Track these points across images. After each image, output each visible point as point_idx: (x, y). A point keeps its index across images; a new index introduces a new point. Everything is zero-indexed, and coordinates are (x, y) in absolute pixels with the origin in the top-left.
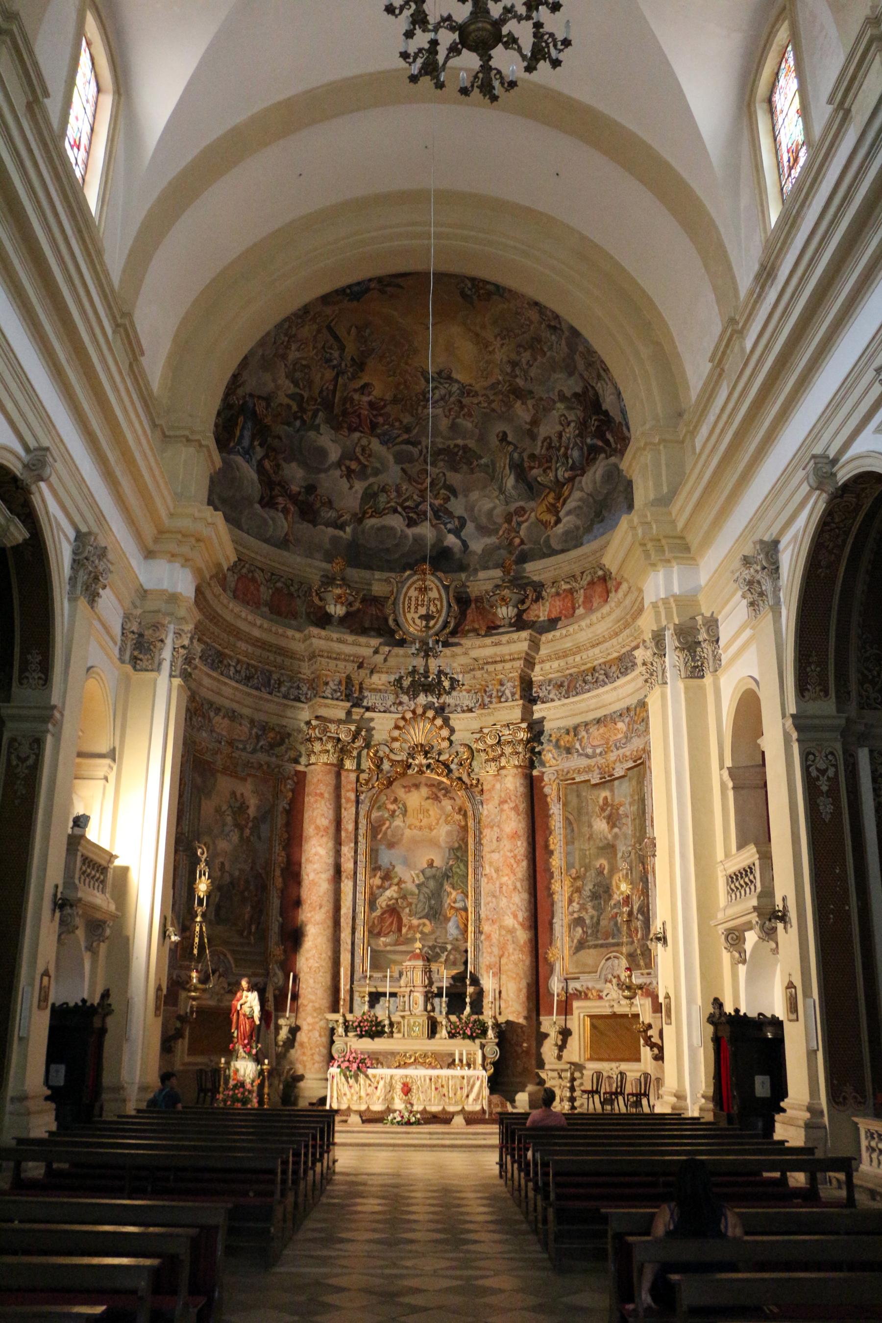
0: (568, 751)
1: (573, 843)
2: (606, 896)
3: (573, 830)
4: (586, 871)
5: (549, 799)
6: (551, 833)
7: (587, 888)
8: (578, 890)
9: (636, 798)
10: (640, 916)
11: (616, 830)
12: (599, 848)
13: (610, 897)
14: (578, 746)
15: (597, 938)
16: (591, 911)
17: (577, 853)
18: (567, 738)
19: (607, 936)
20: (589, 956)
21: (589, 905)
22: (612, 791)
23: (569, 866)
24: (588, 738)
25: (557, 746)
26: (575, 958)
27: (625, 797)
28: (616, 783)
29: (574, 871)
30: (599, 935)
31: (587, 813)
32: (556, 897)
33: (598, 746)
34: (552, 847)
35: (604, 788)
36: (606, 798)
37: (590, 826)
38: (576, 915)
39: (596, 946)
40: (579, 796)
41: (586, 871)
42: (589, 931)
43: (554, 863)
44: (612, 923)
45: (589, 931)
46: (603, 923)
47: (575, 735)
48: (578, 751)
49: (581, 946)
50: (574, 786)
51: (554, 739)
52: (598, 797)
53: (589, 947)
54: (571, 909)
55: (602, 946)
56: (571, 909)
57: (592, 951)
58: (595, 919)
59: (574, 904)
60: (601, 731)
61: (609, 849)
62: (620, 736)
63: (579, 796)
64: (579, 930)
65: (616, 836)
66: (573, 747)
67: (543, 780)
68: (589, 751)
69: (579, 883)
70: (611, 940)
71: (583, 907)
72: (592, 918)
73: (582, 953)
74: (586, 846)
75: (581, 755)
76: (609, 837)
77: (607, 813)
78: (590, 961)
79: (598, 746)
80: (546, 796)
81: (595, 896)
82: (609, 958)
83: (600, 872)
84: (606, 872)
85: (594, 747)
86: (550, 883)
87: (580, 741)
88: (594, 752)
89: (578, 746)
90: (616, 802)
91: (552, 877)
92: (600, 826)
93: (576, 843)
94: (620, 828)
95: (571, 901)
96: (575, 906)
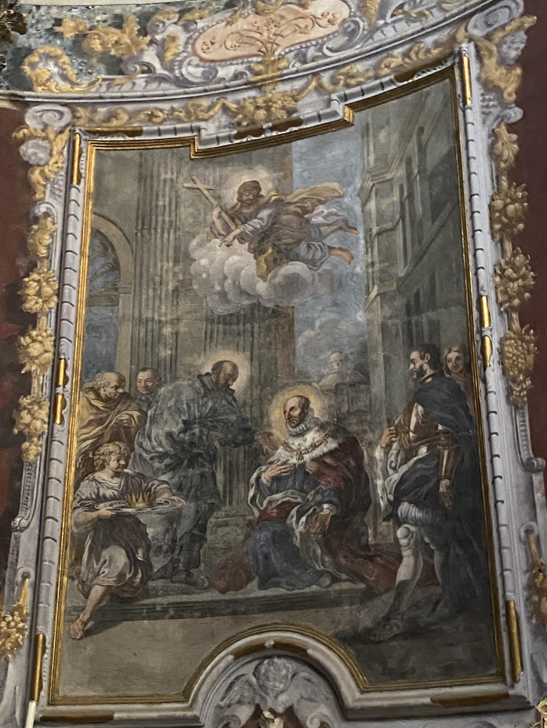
0: (116, 66)
1: (114, 302)
2: (240, 454)
3: (115, 267)
4: (158, 380)
5: (36, 176)
6: (32, 267)
7: (158, 432)
8: (123, 434)
9: (398, 173)
10: (405, 508)
11: (296, 267)
12: (210, 320)
13: (257, 457)
14: (150, 56)
15: (192, 584)
16: (168, 499)
17: (126, 331)
18: (114, 35)
19: (237, 575)
20: (151, 645)
21: (163, 482)
22: (282, 168)
23: (92, 365)
24: (190, 41)
25: (78, 47)
26: (90, 646)
27: (344, 178)
28: (298, 146)
29: (112, 378)
30: (200, 574)
31: (174, 226)
32: (33, 450)
33: (226, 62)
34: (32, 304)
35: (249, 165)
36: (256, 186)
37: (183, 257)
38: (104, 510)
39: (181, 611)
40: (144, 178)
41: (158, 380)
42: (158, 563)
43: (35, 349)
44: (262, 536)
45: (158, 563)
46: (225, 533)
47: (143, 32)
48: (149, 69)
49: (120, 605)
50: (131, 154)
51: (68, 30)
52: (221, 183)
53: (153, 614)
54: (87, 489)
55: (208, 610)
56: (87, 489)
57: (171, 628)
58: (185, 525)
59: (103, 476)
60: (241, 24)
61: (265, 324)
62: (317, 33)
63: (144, 178)
64: (119, 558)
65: (293, 283)
66: (136, 60)
67: (21, 123)
68: (192, 71)
69: (128, 414)
70: (254, 591)
71: (135, 486)
72: (172, 519)
73: (122, 630)
74: (165, 311)
75: (162, 79)
76: (262, 287)
77: (255, 223)
78: (155, 661)
79: (226, 62)
80: (28, 166)
81: (186, 454)
82: (259, 648)
83: (218, 384)
84: (237, 386)
85: (211, 65)
86: (18, 408)
87: (161, 48)
88: (210, 76)
89: (150, 56)
90: (299, 191)
91: (27, 391)
92: (226, 260)
93: (125, 305)
94: (312, 263)
95: (88, 465)
96: (107, 480)
